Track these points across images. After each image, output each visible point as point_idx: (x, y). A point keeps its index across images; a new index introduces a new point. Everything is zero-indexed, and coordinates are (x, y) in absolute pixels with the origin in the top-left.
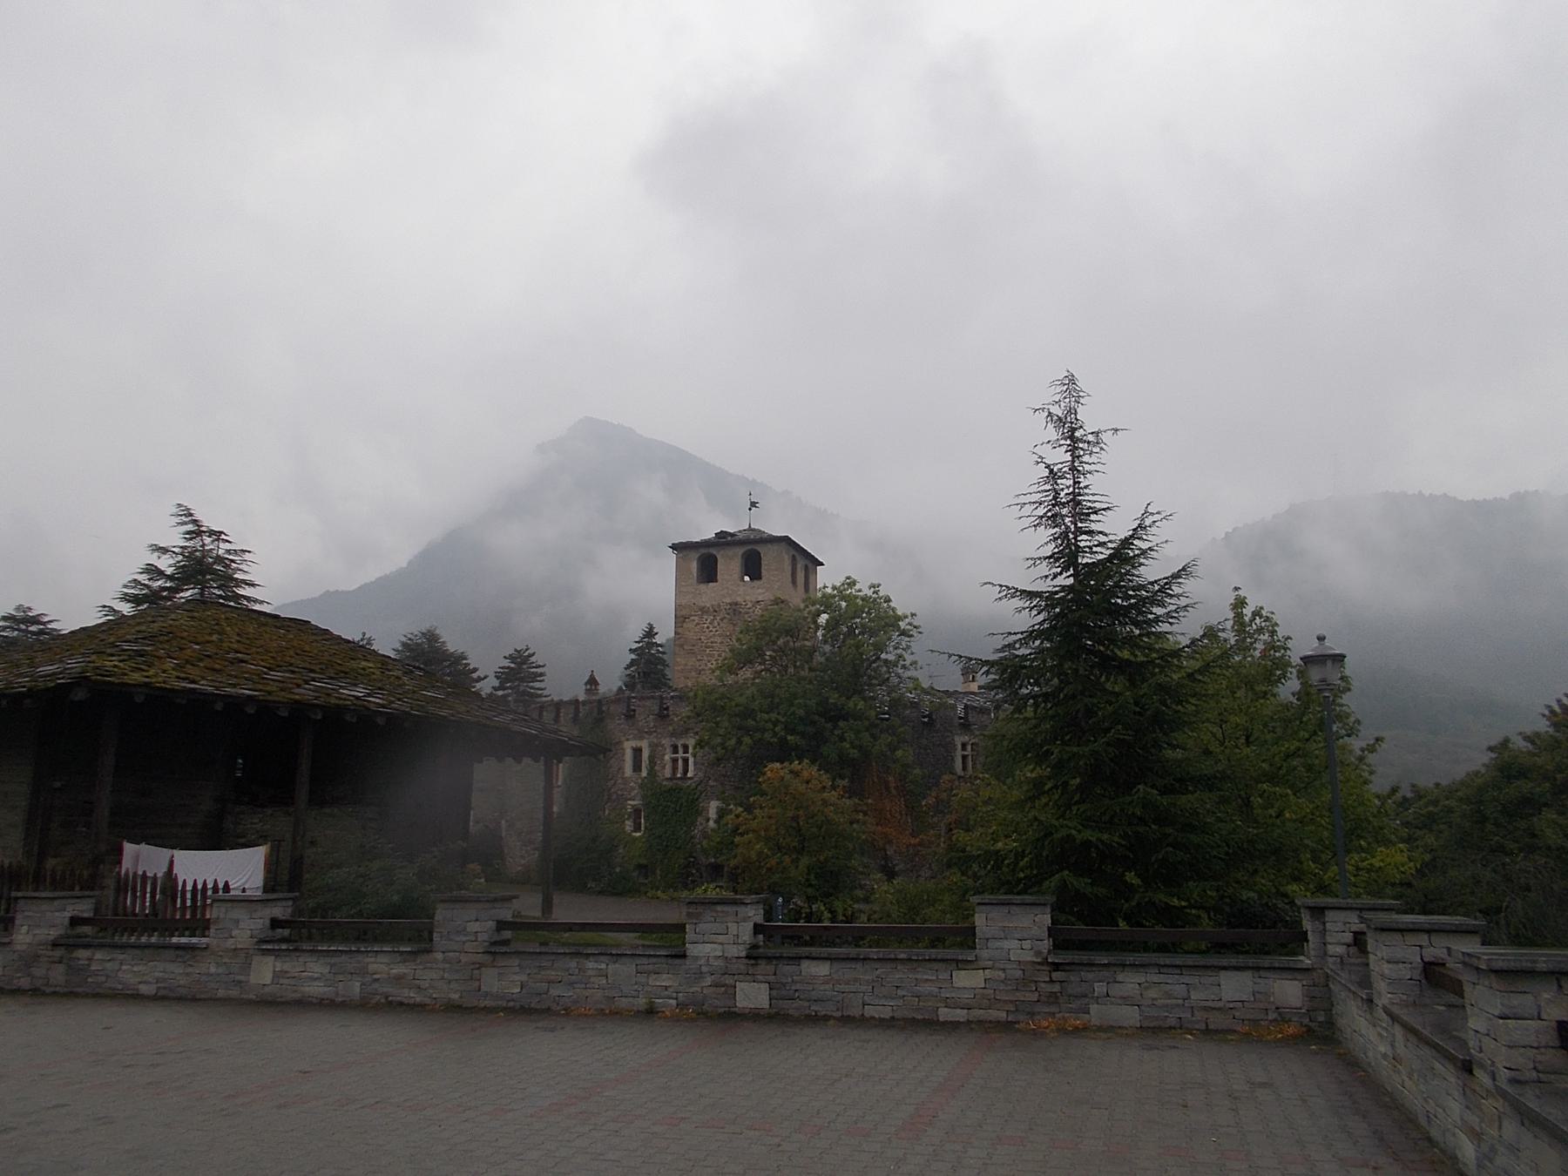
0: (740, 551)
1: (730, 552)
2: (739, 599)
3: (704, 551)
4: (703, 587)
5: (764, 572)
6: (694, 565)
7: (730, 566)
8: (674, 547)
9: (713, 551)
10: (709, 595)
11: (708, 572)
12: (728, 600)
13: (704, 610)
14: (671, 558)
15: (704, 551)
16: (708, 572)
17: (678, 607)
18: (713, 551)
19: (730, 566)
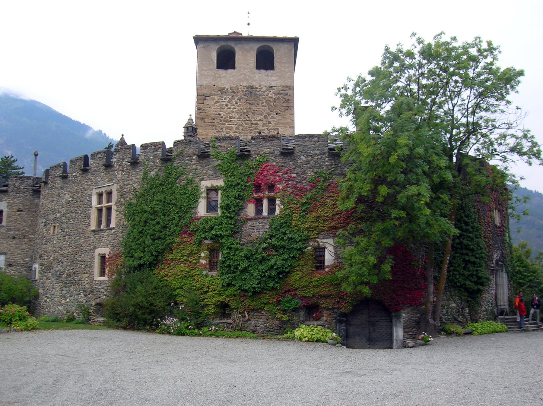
0: (256, 46)
1: (247, 46)
2: (254, 84)
3: (223, 43)
4: (222, 72)
5: (276, 64)
6: (214, 56)
7: (245, 59)
8: (199, 40)
9: (232, 44)
10: (227, 78)
11: (226, 60)
12: (245, 84)
13: (223, 91)
14: (192, 50)
15: (223, 43)
16: (226, 60)
17: (200, 87)
18: (232, 44)
19: (245, 59)
